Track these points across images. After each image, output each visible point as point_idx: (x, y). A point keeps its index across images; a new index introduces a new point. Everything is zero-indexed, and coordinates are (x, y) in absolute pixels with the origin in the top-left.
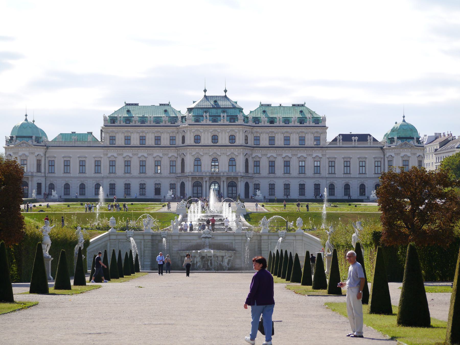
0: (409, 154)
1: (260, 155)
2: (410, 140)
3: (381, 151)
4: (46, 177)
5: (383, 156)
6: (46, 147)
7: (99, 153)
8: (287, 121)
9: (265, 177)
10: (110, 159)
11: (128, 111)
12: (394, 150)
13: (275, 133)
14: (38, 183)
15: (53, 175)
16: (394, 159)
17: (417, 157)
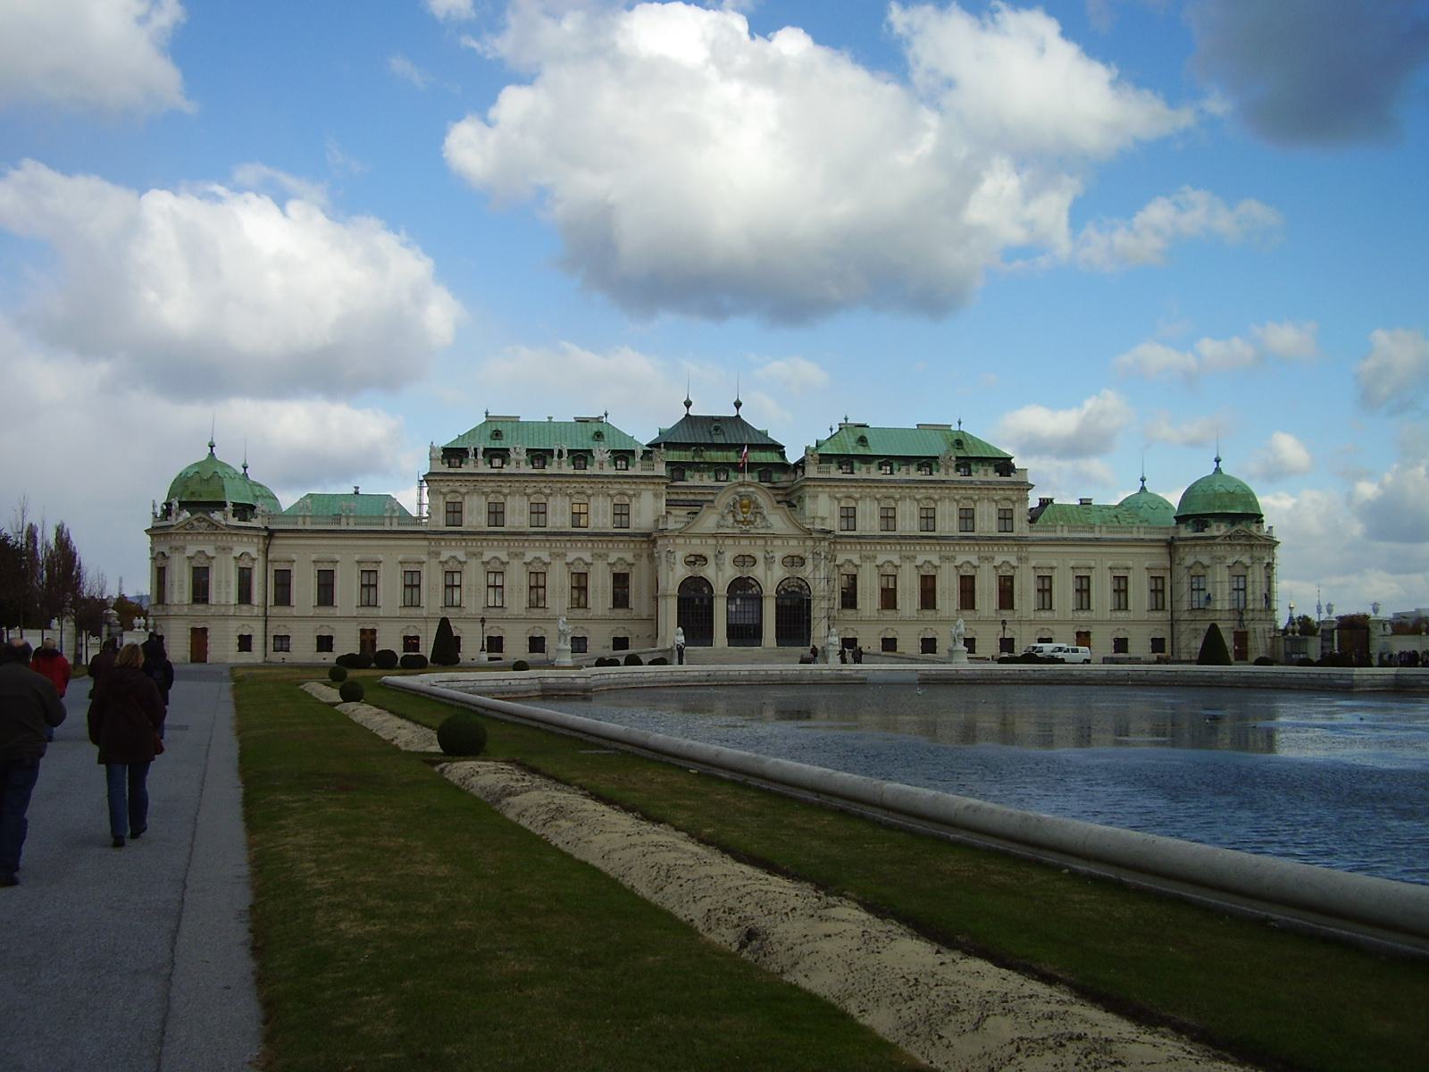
0: (1246, 560)
1: (857, 562)
2: (1244, 523)
3: (1163, 550)
4: (266, 618)
5: (1168, 564)
6: (265, 534)
7: (415, 550)
8: (927, 463)
9: (869, 622)
10: (447, 568)
11: (497, 434)
12: (1209, 548)
13: (896, 501)
14: (241, 637)
15: (285, 610)
16: (1209, 571)
17: (1265, 568)
